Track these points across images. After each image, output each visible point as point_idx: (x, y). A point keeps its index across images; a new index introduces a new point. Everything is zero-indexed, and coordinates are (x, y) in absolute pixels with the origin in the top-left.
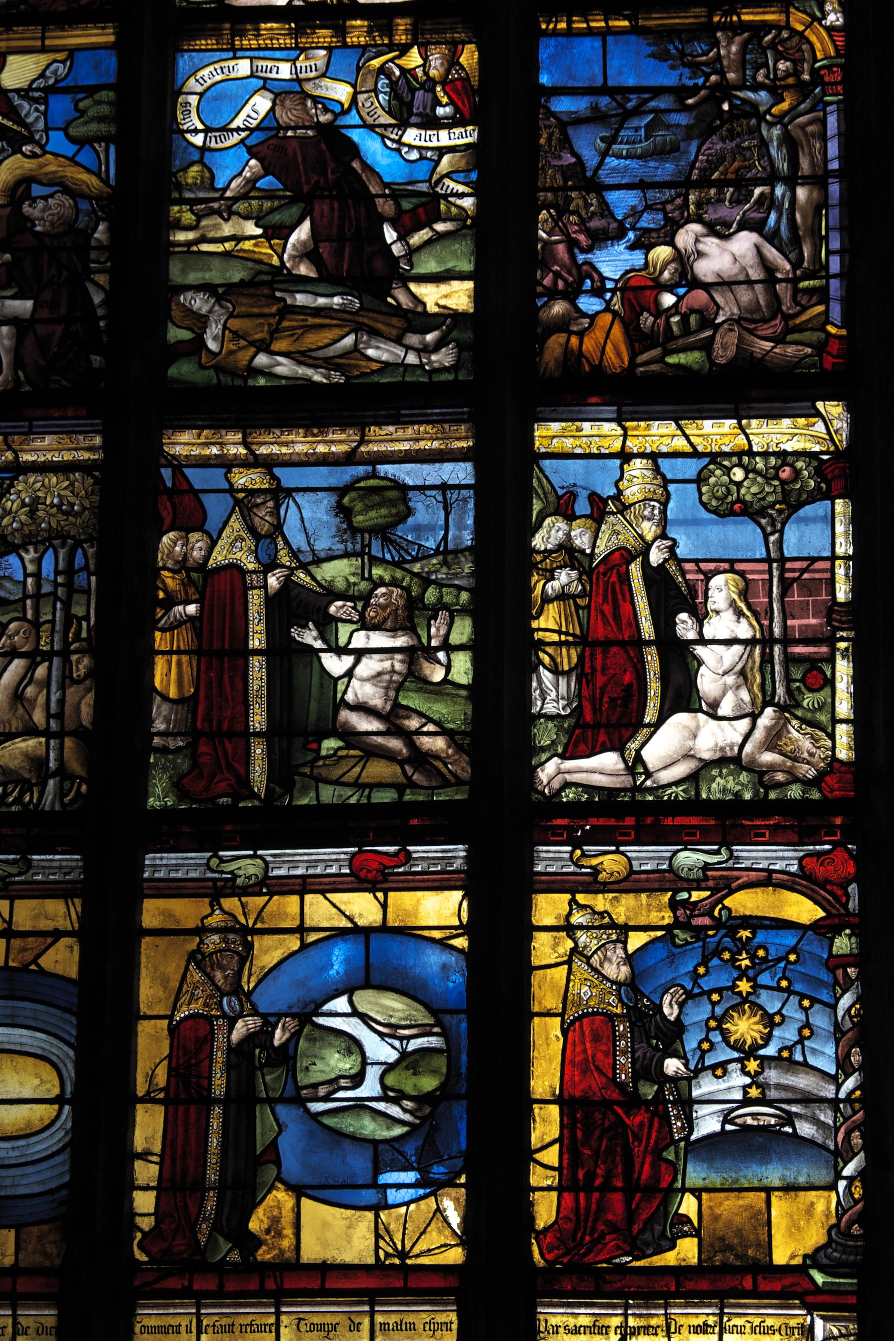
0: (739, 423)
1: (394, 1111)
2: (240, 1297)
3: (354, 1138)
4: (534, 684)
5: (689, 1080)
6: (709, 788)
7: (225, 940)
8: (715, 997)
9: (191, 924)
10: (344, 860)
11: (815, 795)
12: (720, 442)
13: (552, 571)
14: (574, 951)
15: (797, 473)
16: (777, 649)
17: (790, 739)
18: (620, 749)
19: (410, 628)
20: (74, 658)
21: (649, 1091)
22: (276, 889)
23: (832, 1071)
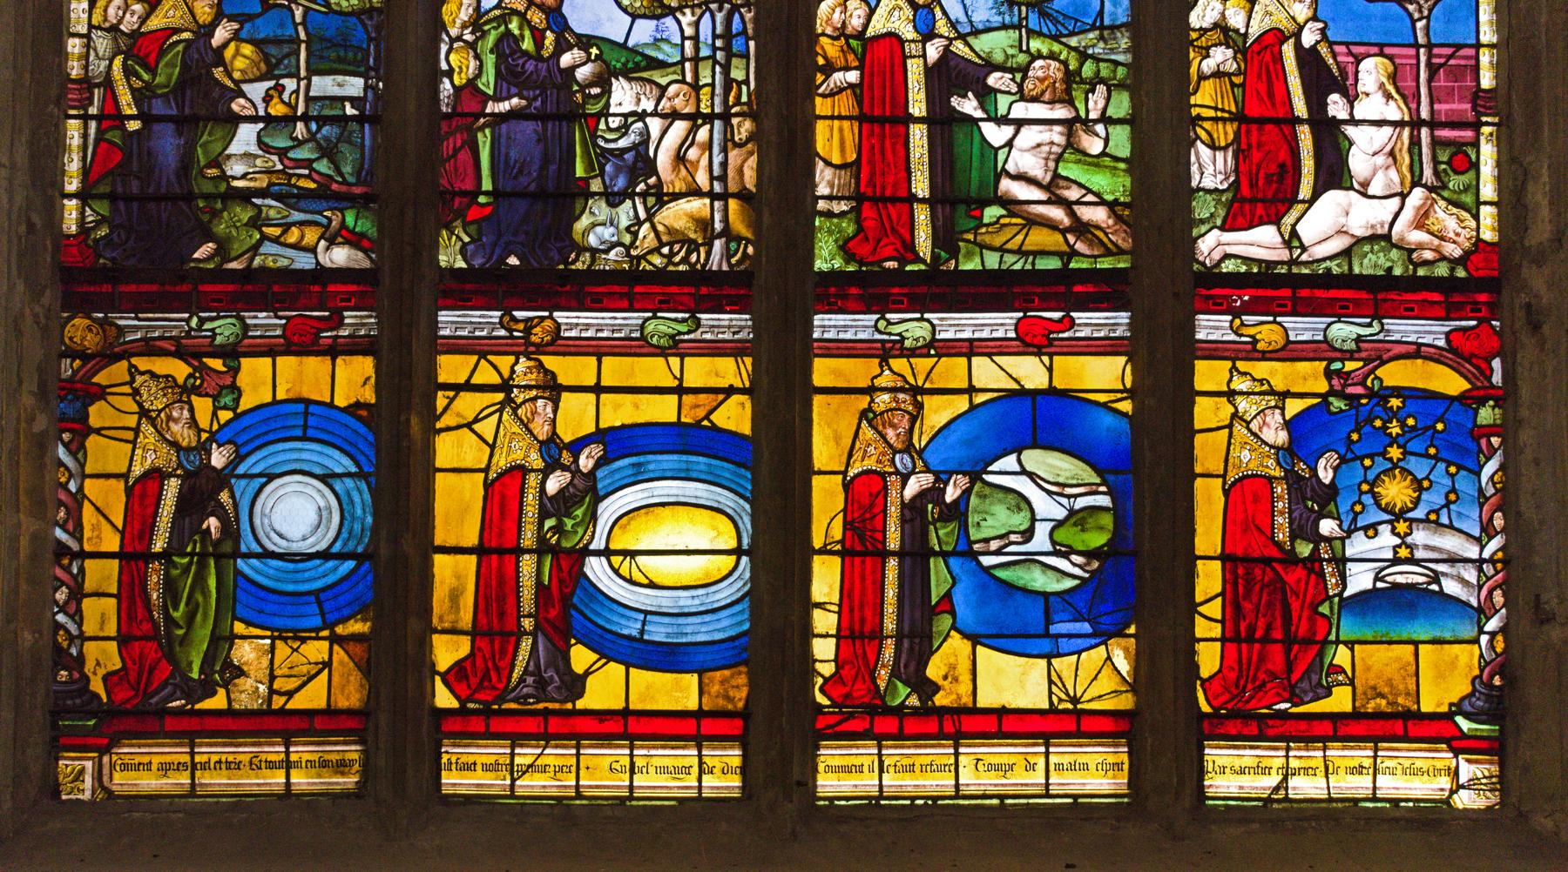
3: (1025, 591)
4: (1193, 158)
5: (1343, 540)
7: (896, 400)
8: (1367, 462)
9: (863, 383)
11: (1461, 273)
13: (1208, 48)
14: (1235, 415)
16: (1424, 132)
18: (1276, 221)
19: (1070, 102)
20: (735, 121)
21: (1304, 549)
23: (1477, 534)
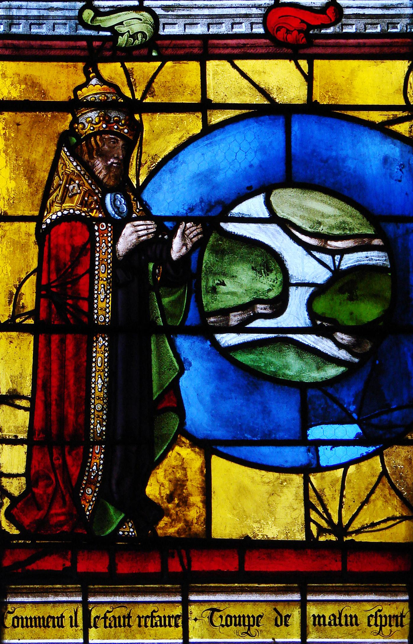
1: (326, 346)
2: (136, 583)
7: (106, 119)
9: (61, 95)
10: (256, 16)
22: (169, 52)
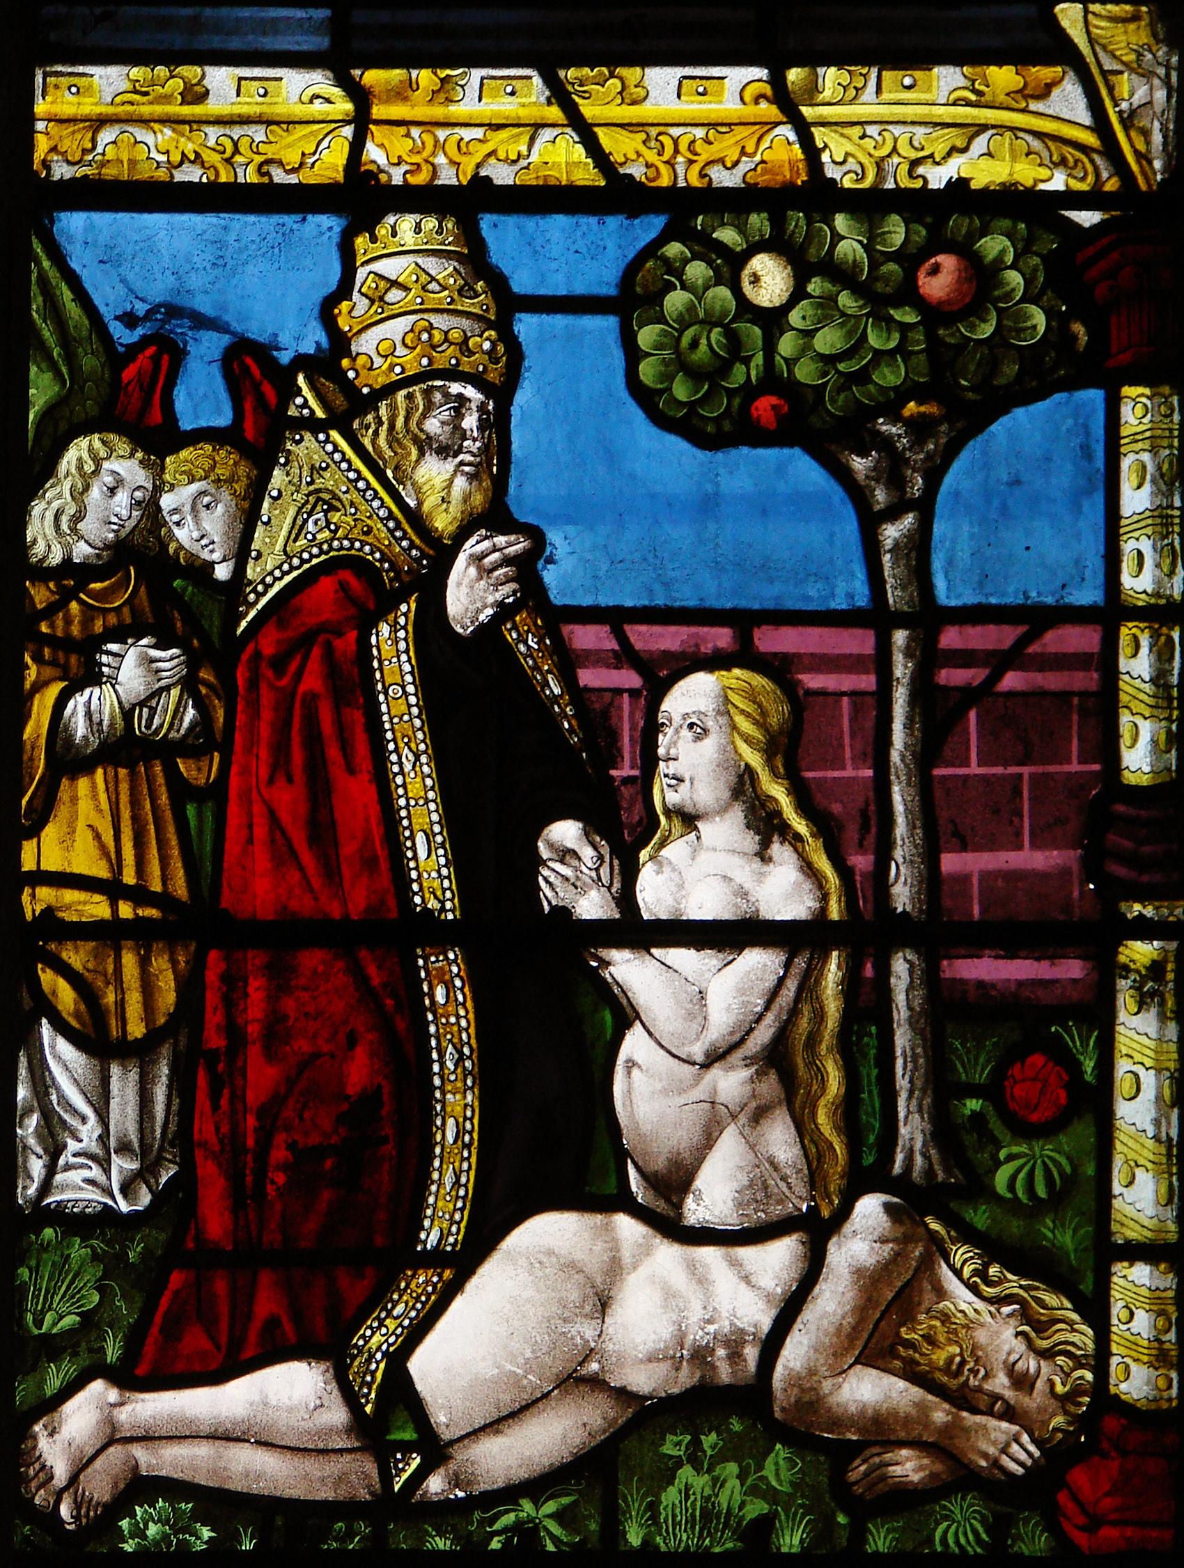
0: (777, 81)
4: (22, 1093)
6: (653, 1507)
12: (705, 153)
13: (90, 646)
15: (982, 278)
17: (945, 1318)
18: (329, 1345)
